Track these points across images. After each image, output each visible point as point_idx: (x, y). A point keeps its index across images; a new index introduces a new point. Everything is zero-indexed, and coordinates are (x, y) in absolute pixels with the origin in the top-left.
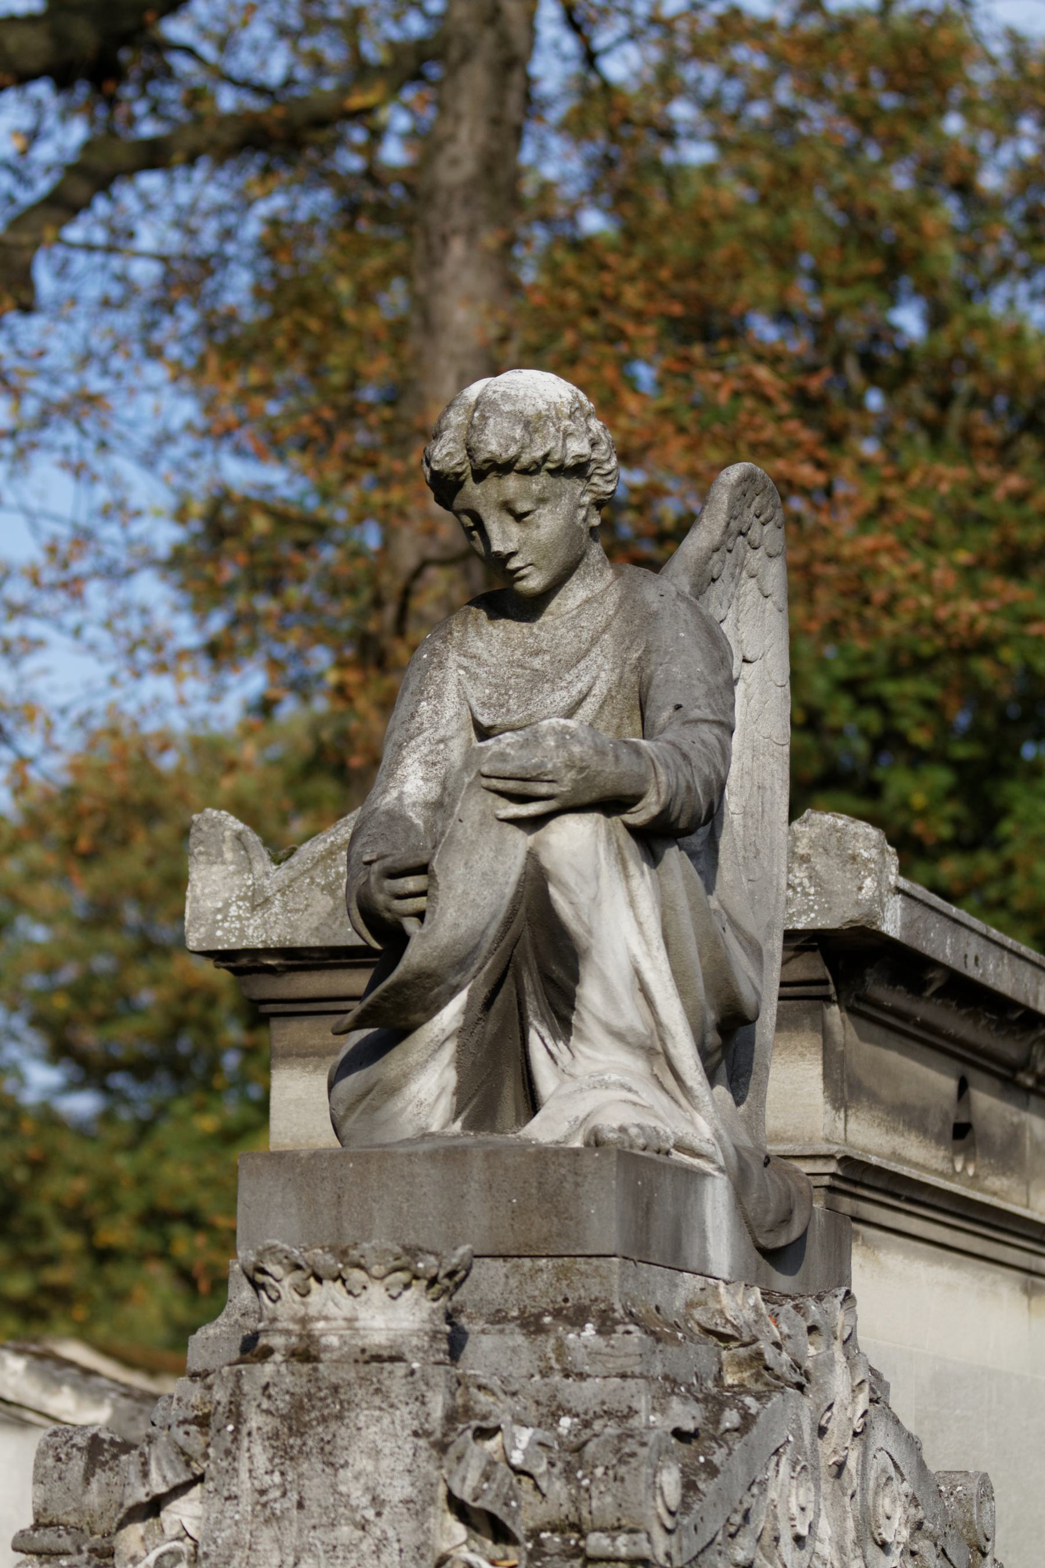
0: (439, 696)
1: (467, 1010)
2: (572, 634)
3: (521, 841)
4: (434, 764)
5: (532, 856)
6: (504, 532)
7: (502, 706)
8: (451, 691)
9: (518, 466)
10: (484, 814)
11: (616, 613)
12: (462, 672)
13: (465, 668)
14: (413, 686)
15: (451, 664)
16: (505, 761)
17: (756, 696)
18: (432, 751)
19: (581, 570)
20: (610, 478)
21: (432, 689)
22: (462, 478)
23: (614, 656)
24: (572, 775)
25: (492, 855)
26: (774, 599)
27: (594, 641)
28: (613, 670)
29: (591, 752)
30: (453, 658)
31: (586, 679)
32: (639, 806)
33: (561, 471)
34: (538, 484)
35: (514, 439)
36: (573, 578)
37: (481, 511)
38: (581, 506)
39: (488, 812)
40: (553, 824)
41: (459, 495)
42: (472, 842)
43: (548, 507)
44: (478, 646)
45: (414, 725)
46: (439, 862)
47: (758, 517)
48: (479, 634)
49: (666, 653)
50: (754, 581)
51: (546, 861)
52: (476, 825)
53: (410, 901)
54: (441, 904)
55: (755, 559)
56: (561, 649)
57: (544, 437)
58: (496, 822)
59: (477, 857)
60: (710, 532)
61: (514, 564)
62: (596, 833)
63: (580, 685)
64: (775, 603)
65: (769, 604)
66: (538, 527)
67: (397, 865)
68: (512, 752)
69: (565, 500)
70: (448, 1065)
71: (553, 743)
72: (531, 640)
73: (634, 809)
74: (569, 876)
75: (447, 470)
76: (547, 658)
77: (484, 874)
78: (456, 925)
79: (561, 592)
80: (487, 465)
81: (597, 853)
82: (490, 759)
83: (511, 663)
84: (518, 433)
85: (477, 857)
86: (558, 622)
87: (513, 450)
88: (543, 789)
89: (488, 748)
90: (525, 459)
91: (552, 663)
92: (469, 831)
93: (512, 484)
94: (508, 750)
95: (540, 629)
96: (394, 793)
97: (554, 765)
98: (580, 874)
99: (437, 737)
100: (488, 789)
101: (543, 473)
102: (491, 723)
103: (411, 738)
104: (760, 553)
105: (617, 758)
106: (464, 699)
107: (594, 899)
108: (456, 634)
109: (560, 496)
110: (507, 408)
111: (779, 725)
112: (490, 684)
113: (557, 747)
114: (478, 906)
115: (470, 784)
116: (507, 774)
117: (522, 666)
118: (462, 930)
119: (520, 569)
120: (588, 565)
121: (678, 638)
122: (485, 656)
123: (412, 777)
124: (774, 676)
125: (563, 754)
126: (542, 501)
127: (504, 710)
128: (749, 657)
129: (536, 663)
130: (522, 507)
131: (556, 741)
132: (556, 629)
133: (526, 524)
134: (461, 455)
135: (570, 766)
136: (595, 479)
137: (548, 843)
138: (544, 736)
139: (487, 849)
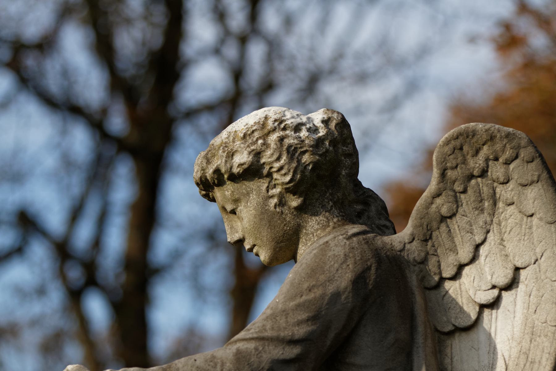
6: (232, 227)
17: (533, 293)
20: (283, 172)
26: (538, 216)
33: (234, 178)
38: (272, 197)
43: (243, 204)
47: (496, 159)
50: (512, 207)
55: (505, 192)
64: (541, 219)
65: (535, 220)
69: (253, 197)
104: (511, 185)
109: (248, 194)
120: (307, 234)
124: (549, 275)
126: (237, 201)
128: (519, 265)
130: (229, 207)
136: (275, 176)
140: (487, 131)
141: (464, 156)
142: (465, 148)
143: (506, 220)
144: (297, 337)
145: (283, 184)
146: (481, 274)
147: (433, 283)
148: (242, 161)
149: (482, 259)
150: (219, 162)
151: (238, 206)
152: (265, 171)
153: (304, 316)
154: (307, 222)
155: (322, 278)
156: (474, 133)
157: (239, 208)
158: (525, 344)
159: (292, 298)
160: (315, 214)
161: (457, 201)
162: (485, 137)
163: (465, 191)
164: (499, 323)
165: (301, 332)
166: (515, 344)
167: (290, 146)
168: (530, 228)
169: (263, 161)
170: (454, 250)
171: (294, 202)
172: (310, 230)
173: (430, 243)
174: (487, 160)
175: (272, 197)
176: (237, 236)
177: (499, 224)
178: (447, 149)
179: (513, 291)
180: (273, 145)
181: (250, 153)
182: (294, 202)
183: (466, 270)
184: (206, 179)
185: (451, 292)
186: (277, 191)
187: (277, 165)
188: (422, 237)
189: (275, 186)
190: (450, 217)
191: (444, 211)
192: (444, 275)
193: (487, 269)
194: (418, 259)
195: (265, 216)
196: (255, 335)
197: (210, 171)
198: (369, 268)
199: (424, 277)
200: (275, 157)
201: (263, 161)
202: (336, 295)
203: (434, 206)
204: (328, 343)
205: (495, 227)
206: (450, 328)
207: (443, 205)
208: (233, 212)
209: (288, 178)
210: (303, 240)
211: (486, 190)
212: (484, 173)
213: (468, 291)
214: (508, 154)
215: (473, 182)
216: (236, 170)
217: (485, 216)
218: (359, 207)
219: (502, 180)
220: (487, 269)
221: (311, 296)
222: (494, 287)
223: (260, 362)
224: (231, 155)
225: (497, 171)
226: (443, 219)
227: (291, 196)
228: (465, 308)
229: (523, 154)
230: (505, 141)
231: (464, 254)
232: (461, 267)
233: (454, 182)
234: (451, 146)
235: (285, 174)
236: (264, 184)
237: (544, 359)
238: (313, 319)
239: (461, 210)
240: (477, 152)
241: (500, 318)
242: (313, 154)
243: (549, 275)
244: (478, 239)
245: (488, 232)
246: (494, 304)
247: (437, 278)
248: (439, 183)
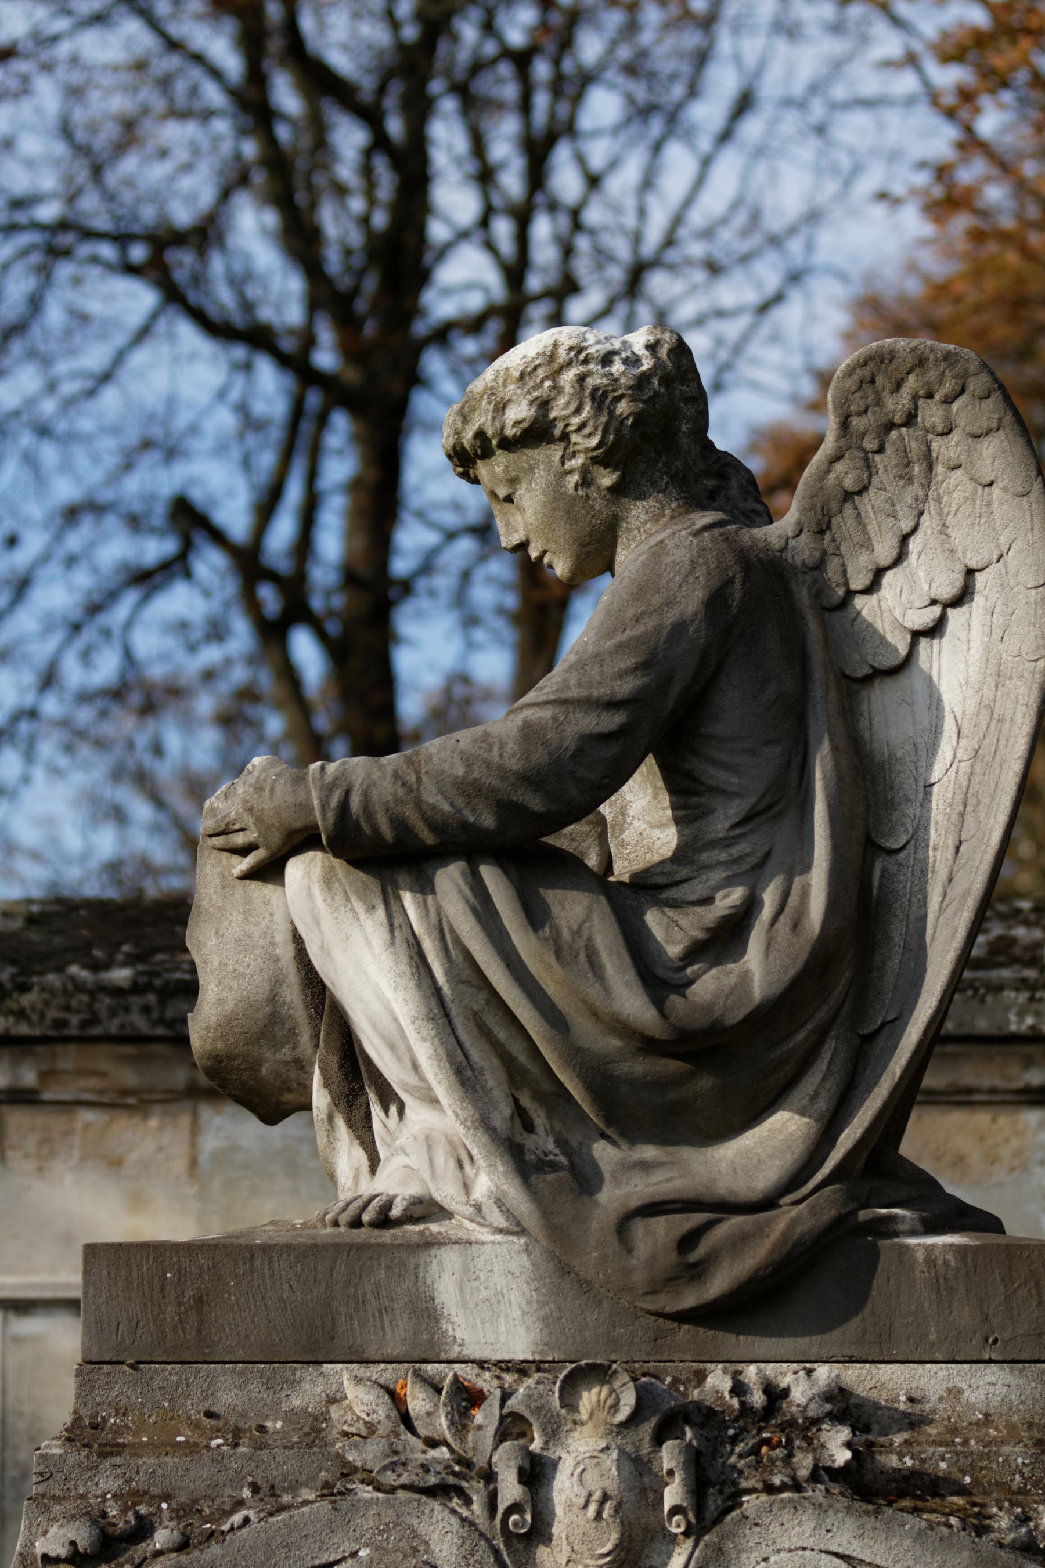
1: (327, 1084)
6: (507, 524)
10: (222, 875)
17: (998, 610)
20: (586, 431)
25: (240, 918)
26: (1001, 485)
33: (507, 444)
38: (571, 472)
39: (227, 874)
43: (524, 485)
47: (930, 396)
50: (959, 472)
52: (219, 889)
55: (945, 449)
62: (308, 874)
64: (1005, 489)
65: (996, 491)
69: (540, 473)
70: (351, 1144)
77: (238, 940)
78: (221, 1001)
81: (310, 895)
88: (239, 839)
92: (214, 897)
104: (955, 437)
105: (272, 791)
107: (322, 947)
109: (531, 469)
111: (1032, 635)
114: (244, 976)
118: (230, 1005)
120: (629, 530)
124: (1021, 578)
126: (513, 481)
128: (973, 564)
130: (502, 492)
136: (574, 438)
140: (913, 350)
141: (877, 393)
142: (879, 380)
143: (950, 493)
144: (619, 697)
145: (587, 450)
146: (913, 583)
147: (835, 600)
148: (520, 417)
149: (913, 557)
150: (483, 419)
151: (516, 489)
152: (557, 432)
153: (629, 662)
154: (628, 510)
155: (656, 600)
156: (892, 355)
157: (518, 493)
158: (988, 693)
159: (610, 634)
160: (642, 497)
161: (869, 467)
162: (910, 361)
163: (881, 450)
164: (944, 660)
165: (625, 688)
166: (971, 692)
167: (595, 389)
168: (989, 504)
169: (553, 414)
170: (867, 545)
171: (607, 479)
172: (634, 522)
173: (828, 536)
174: (915, 398)
175: (571, 472)
176: (516, 539)
177: (939, 500)
178: (850, 383)
179: (965, 608)
180: (568, 389)
181: (531, 403)
182: (607, 479)
183: (888, 577)
184: (463, 448)
185: (864, 613)
186: (578, 461)
187: (576, 421)
188: (814, 528)
189: (574, 455)
190: (859, 493)
191: (849, 483)
192: (854, 586)
193: (921, 574)
194: (810, 562)
195: (559, 503)
196: (552, 697)
197: (468, 435)
198: (731, 581)
199: (820, 591)
200: (573, 407)
201: (553, 414)
202: (680, 627)
203: (832, 476)
204: (670, 704)
205: (931, 506)
206: (865, 671)
207: (846, 475)
208: (509, 499)
209: (595, 441)
210: (622, 539)
211: (915, 448)
212: (910, 419)
213: (892, 610)
214: (949, 386)
215: (894, 434)
216: (510, 432)
217: (916, 489)
218: (711, 483)
219: (940, 428)
220: (921, 574)
221: (640, 629)
222: (934, 602)
223: (562, 740)
224: (501, 407)
225: (931, 414)
226: (848, 496)
227: (601, 470)
228: (889, 638)
229: (974, 385)
230: (943, 365)
231: (884, 551)
232: (879, 573)
233: (863, 436)
234: (856, 378)
235: (590, 435)
236: (555, 452)
237: (1019, 715)
238: (644, 666)
239: (875, 481)
240: (898, 386)
241: (944, 652)
242: (634, 399)
243: (1021, 578)
244: (906, 526)
245: (921, 514)
246: (936, 630)
247: (841, 592)
248: (838, 438)
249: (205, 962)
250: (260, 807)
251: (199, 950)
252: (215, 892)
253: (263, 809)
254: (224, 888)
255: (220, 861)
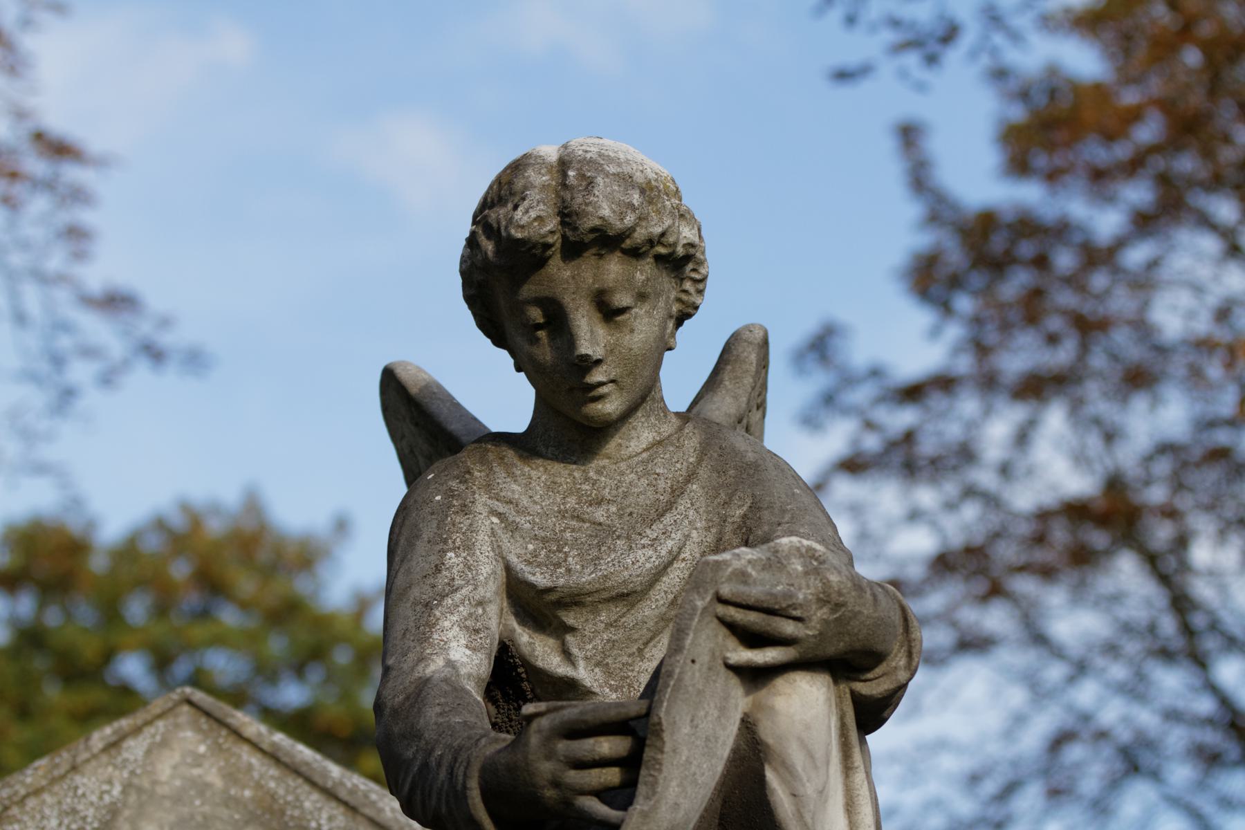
0: (469, 547)
2: (644, 481)
3: (740, 700)
4: (477, 631)
5: (748, 726)
6: (592, 332)
7: (558, 565)
8: (482, 539)
9: (628, 243)
11: (700, 461)
12: (495, 520)
13: (499, 515)
14: (428, 532)
15: (479, 507)
16: (745, 583)
18: (471, 615)
19: (647, 406)
21: (458, 539)
22: (549, 252)
23: (708, 512)
24: (822, 613)
27: (677, 492)
28: (708, 529)
29: (849, 584)
30: (482, 502)
31: (678, 536)
32: (878, 671)
34: (644, 271)
35: (631, 206)
36: (639, 414)
37: (567, 300)
39: (717, 654)
40: (780, 683)
41: (535, 278)
42: (700, 692)
43: (646, 307)
44: (515, 489)
45: (442, 580)
46: (668, 712)
48: (511, 475)
49: (784, 511)
51: (767, 732)
52: (704, 669)
53: (595, 772)
54: (665, 773)
56: (631, 499)
57: (658, 212)
58: (723, 670)
59: (702, 713)
60: (736, 398)
61: (597, 376)
63: (670, 543)
66: (632, 331)
67: (589, 717)
68: (754, 573)
71: (800, 568)
72: (586, 487)
73: (870, 675)
74: (797, 758)
75: (535, 238)
76: (613, 509)
78: (677, 805)
79: (624, 429)
80: (592, 236)
82: (729, 579)
83: (562, 514)
84: (636, 198)
85: (702, 713)
86: (623, 466)
87: (630, 219)
88: (789, 628)
89: (725, 562)
90: (640, 235)
91: (621, 517)
92: (697, 674)
93: (614, 268)
94: (750, 570)
95: (599, 472)
96: (440, 662)
97: (805, 598)
98: (811, 755)
99: (477, 597)
100: (723, 621)
101: (650, 260)
102: (549, 584)
103: (443, 596)
106: (501, 557)
107: (821, 792)
108: (477, 474)
110: (612, 169)
112: (536, 537)
113: (806, 573)
115: (705, 609)
116: (751, 602)
117: (578, 518)
119: (601, 384)
121: (793, 494)
122: (525, 501)
123: (453, 644)
125: (815, 584)
126: (642, 297)
127: (562, 570)
129: (600, 514)
130: (622, 299)
131: (804, 566)
132: (622, 474)
133: (618, 326)
134: (552, 224)
135: (823, 601)
137: (772, 708)
138: (788, 557)
139: (712, 705)
151: (636, 306)
249: (674, 751)
250: (857, 608)
251: (672, 734)
252: (700, 670)
253: (860, 612)
254: (710, 669)
255: (716, 636)
